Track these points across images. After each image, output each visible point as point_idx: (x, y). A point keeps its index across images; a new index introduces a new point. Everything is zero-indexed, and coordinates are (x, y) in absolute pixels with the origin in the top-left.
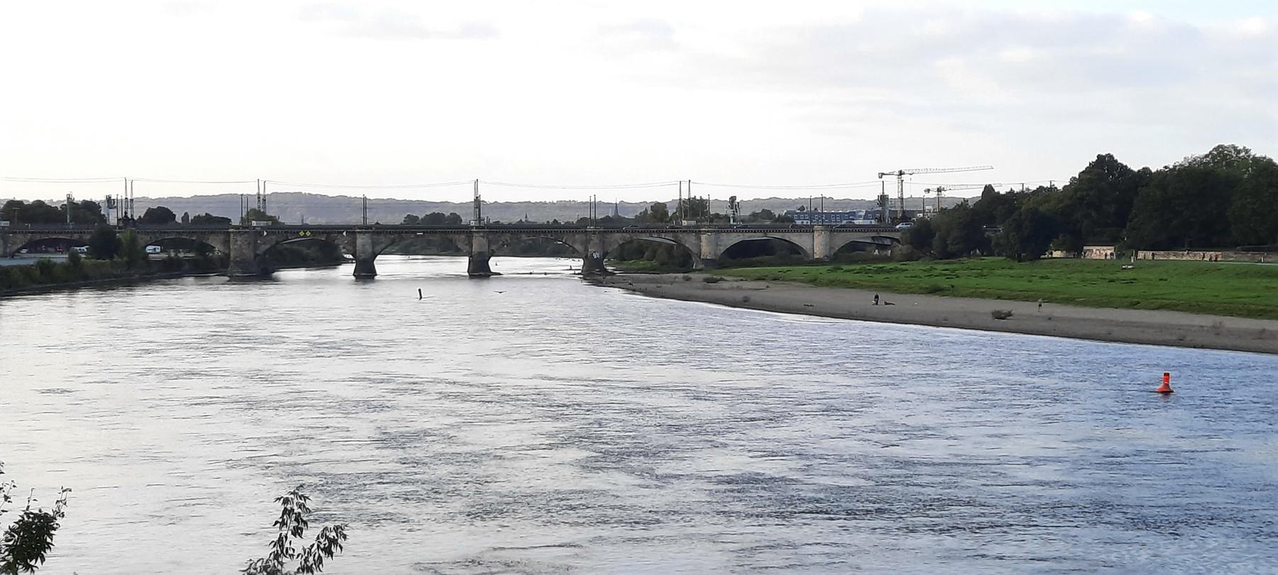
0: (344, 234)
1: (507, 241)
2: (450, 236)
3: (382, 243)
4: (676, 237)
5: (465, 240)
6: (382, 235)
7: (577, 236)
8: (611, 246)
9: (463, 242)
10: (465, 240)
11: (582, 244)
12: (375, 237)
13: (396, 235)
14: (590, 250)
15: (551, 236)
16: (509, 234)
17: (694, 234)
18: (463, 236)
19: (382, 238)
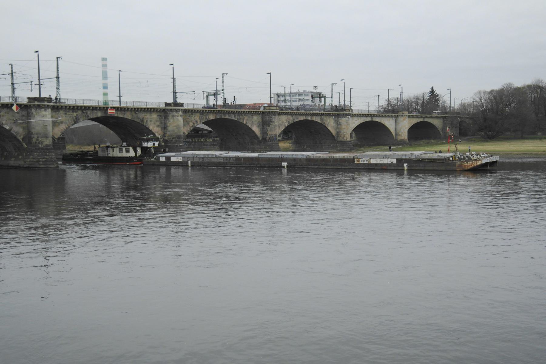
0: (14, 108)
1: (197, 122)
2: (141, 115)
3: (62, 123)
4: (322, 120)
5: (157, 121)
6: (62, 112)
7: (255, 118)
8: (279, 128)
9: (155, 124)
10: (157, 121)
11: (258, 126)
12: (54, 113)
13: (80, 112)
14: (269, 133)
15: (235, 116)
16: (198, 114)
17: (334, 117)
18: (155, 116)
19: (61, 117)
